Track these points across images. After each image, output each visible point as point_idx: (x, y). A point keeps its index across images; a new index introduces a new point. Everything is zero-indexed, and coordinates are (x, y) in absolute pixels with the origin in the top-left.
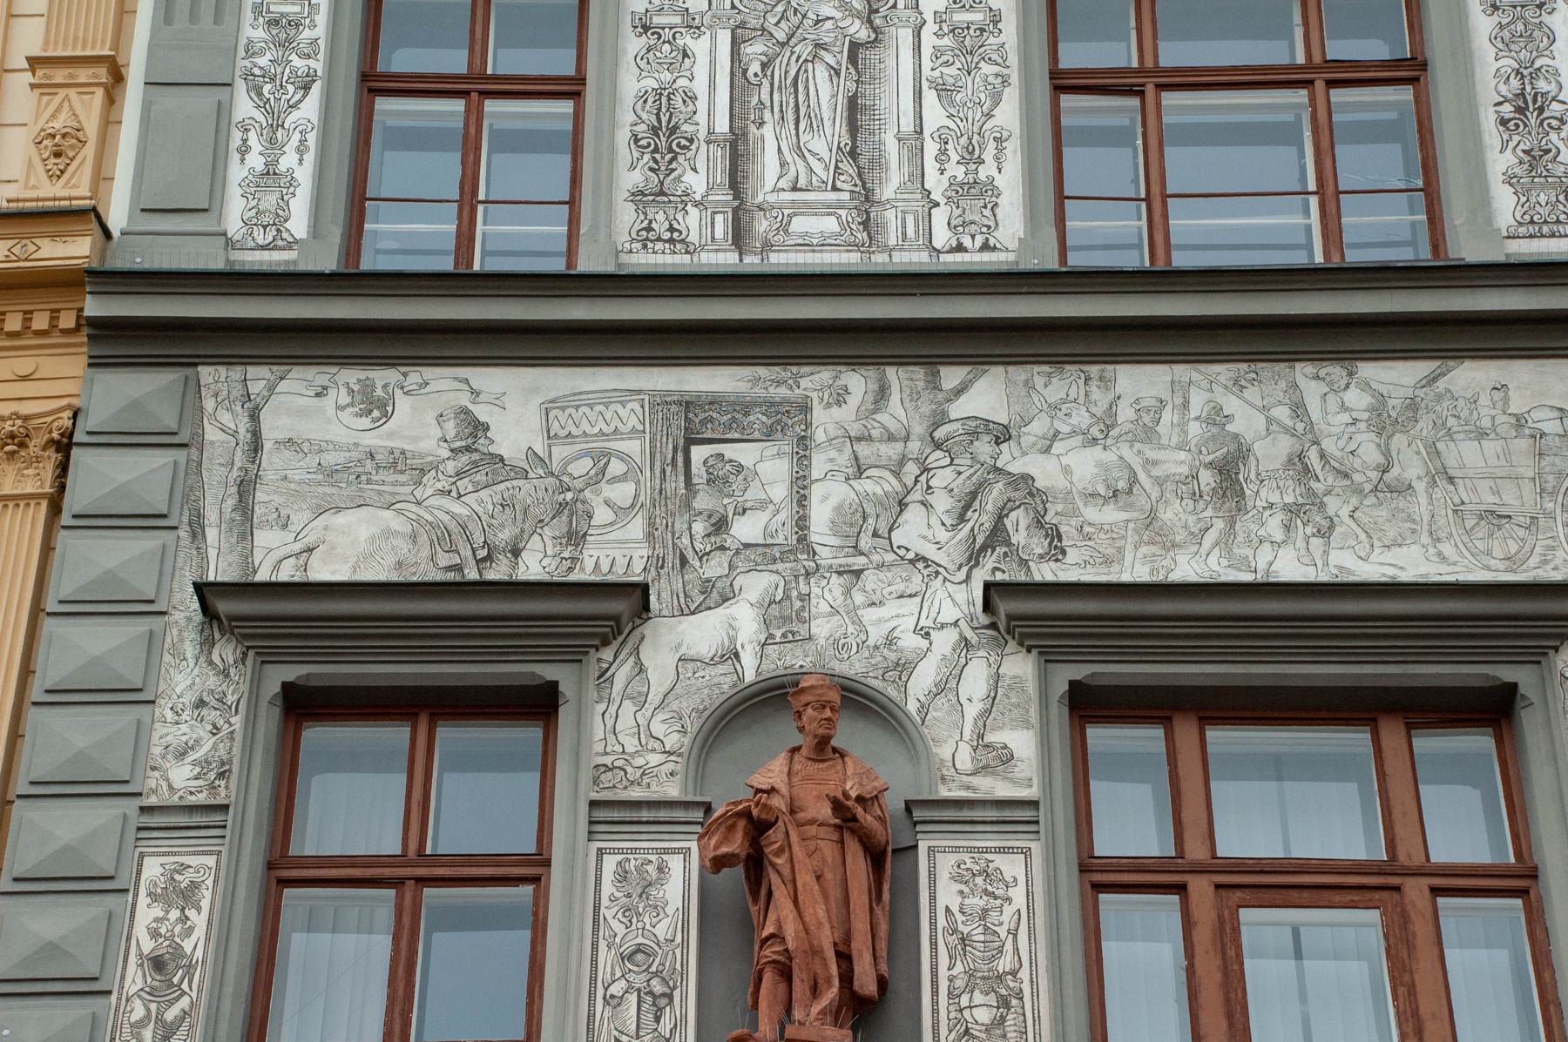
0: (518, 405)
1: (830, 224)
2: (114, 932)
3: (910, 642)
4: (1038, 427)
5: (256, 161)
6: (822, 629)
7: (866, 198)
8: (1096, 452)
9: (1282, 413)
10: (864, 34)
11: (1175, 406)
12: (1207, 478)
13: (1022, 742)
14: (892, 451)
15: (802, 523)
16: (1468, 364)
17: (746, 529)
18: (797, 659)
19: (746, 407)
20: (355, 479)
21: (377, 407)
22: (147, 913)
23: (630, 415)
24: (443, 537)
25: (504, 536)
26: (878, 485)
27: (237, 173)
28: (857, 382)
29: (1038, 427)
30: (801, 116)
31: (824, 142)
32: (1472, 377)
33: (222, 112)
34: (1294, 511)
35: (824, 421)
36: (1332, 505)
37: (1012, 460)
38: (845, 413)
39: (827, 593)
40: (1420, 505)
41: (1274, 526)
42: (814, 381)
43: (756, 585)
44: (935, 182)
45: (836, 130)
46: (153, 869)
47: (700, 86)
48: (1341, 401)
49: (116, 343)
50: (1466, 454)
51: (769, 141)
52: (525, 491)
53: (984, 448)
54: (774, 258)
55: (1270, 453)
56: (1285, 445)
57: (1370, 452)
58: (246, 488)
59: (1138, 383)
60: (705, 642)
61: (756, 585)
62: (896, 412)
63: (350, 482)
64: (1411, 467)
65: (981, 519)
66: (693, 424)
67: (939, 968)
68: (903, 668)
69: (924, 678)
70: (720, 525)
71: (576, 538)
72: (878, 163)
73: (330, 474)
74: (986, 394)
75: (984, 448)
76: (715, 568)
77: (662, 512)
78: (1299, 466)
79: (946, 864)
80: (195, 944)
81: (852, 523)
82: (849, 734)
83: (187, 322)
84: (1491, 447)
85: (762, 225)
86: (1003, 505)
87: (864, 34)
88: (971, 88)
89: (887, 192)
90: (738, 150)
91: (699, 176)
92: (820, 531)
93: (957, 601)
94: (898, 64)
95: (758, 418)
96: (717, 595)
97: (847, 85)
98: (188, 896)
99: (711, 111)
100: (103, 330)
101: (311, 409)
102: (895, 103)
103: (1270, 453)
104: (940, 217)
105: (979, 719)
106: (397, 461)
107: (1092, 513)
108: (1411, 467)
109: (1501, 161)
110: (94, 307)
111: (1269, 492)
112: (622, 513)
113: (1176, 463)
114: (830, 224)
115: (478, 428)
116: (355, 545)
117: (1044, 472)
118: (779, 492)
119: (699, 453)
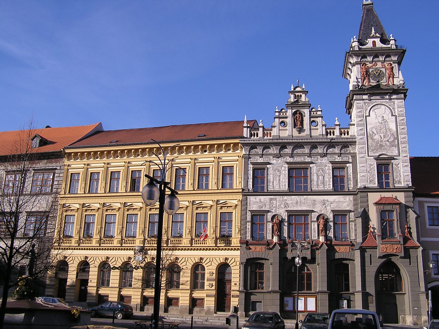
17: (274, 206)
18: (276, 213)
21: (256, 199)
23: (268, 199)
24: (259, 206)
26: (280, 203)
28: (279, 197)
30: (276, 180)
32: (309, 197)
35: (277, 199)
42: (277, 197)
43: (274, 209)
50: (308, 201)
55: (299, 201)
59: (293, 197)
61: (274, 209)
62: (281, 199)
64: (305, 202)
66: (271, 199)
74: (285, 197)
80: (250, 228)
81: (279, 205)
86: (286, 205)
88: (285, 178)
90: (273, 182)
91: (271, 184)
93: (284, 210)
99: (272, 180)
101: (252, 199)
102: (281, 179)
103: (299, 201)
108: (305, 202)
113: (294, 202)
116: (255, 208)
117: (288, 202)
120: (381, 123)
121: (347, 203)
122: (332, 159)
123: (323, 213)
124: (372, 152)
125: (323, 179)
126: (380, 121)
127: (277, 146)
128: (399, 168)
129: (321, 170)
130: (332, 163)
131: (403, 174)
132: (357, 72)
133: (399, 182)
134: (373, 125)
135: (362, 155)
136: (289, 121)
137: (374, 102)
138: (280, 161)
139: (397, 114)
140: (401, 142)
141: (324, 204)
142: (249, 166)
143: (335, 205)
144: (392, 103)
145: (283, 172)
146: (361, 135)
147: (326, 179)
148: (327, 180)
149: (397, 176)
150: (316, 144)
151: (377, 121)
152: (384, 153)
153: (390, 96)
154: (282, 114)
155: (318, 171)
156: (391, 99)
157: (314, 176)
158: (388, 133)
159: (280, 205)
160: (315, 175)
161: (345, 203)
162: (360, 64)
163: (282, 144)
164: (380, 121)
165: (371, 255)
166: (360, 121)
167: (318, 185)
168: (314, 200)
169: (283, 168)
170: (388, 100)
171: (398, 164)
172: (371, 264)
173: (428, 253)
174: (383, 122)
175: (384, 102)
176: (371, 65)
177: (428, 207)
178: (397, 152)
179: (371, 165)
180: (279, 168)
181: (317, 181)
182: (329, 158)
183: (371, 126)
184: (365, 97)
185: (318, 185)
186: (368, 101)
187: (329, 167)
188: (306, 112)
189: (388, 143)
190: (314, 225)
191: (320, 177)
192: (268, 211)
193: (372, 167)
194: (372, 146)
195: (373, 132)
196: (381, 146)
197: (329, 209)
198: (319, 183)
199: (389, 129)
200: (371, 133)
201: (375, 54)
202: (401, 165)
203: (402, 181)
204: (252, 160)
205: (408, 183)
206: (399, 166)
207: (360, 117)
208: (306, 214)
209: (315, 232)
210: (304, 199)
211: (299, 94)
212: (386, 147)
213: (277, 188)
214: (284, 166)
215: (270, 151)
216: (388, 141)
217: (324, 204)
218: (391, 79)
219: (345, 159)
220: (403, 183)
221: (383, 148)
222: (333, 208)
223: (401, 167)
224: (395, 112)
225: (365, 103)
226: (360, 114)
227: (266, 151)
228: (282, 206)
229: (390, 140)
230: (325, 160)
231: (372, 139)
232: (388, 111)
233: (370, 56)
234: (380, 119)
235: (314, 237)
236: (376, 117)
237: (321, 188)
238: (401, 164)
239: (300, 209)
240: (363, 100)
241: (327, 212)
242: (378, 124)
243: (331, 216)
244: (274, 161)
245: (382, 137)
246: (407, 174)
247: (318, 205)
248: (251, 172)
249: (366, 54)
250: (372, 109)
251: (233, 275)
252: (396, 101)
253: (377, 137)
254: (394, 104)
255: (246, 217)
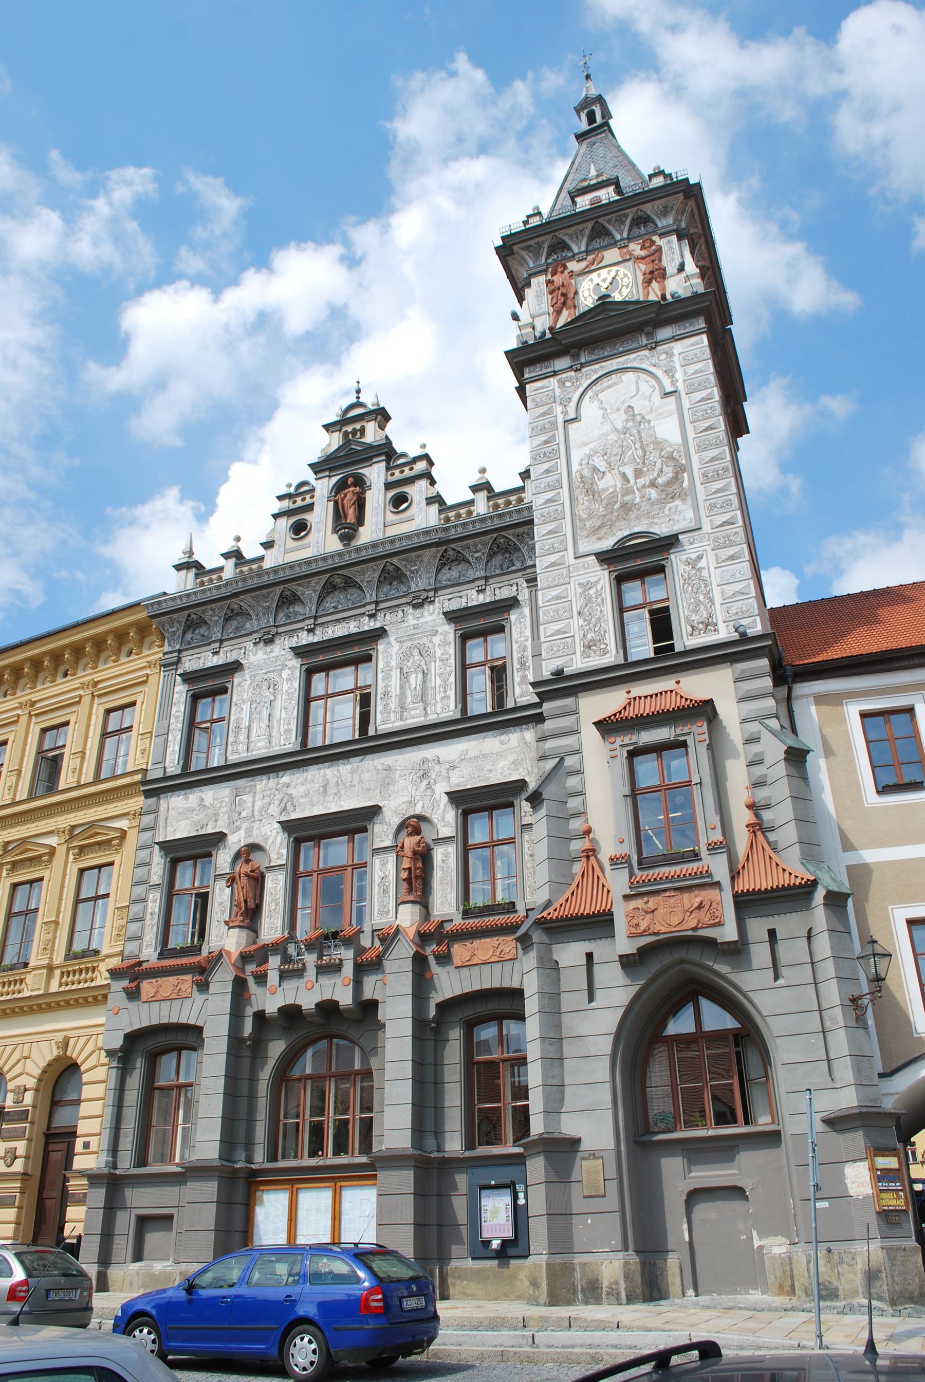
0: (209, 794)
1: (263, 743)
2: (145, 908)
3: (269, 833)
4: (294, 783)
5: (171, 749)
6: (254, 833)
7: (270, 736)
8: (304, 787)
9: (336, 772)
10: (272, 698)
11: (318, 775)
12: (322, 789)
13: (284, 851)
14: (269, 792)
15: (253, 811)
16: (369, 757)
17: (244, 814)
19: (246, 787)
20: (184, 814)
22: (150, 904)
24: (196, 824)
25: (205, 822)
27: (168, 752)
29: (294, 783)
30: (260, 720)
31: (264, 725)
33: (167, 741)
34: (335, 794)
36: (342, 792)
37: (290, 791)
38: (262, 786)
39: (256, 825)
40: (356, 789)
41: (331, 799)
43: (245, 825)
44: (282, 730)
45: (266, 721)
46: (151, 897)
47: (244, 716)
48: (345, 769)
49: (148, 794)
50: (366, 776)
51: (255, 726)
52: (210, 812)
53: (285, 788)
54: (254, 753)
55: (333, 781)
56: (336, 779)
57: (350, 779)
58: (166, 819)
60: (236, 840)
61: (245, 825)
63: (182, 815)
64: (356, 782)
65: (283, 805)
67: (267, 898)
68: (267, 839)
69: (270, 841)
70: (240, 814)
71: (216, 820)
72: (273, 728)
73: (179, 813)
74: (286, 778)
75: (285, 788)
76: (238, 823)
77: (231, 811)
78: (337, 784)
79: (270, 878)
80: (157, 910)
82: (256, 857)
83: (157, 788)
84: (370, 774)
85: (252, 746)
86: (288, 801)
87: (272, 698)
89: (273, 734)
90: (249, 729)
91: (242, 737)
92: (256, 813)
94: (278, 704)
95: (248, 789)
96: (238, 828)
97: (269, 711)
98: (155, 901)
99: (245, 723)
100: (144, 791)
101: (176, 802)
102: (277, 714)
103: (333, 781)
104: (282, 738)
105: (277, 848)
106: (190, 810)
107: (302, 800)
108: (356, 782)
109: (379, 708)
110: (142, 788)
111: (331, 791)
112: (224, 814)
113: (316, 787)
114: (263, 743)
115: (203, 799)
116: (180, 830)
118: (250, 805)
119: (238, 798)
120: (625, 431)
121: (511, 758)
122: (455, 605)
123: (418, 810)
124: (593, 539)
125: (424, 682)
126: (619, 426)
127: (266, 597)
128: (705, 573)
129: (416, 652)
130: (452, 617)
131: (722, 592)
132: (537, 296)
133: (709, 624)
134: (592, 446)
135: (553, 558)
136: (321, 517)
137: (595, 372)
138: (275, 653)
139: (680, 386)
140: (705, 475)
141: (424, 775)
142: (177, 689)
143: (466, 773)
144: (663, 356)
145: (286, 686)
146: (549, 488)
147: (435, 681)
148: (439, 682)
149: (698, 603)
150: (395, 560)
151: (608, 427)
152: (637, 530)
153: (650, 335)
154: (299, 499)
155: (407, 655)
156: (657, 344)
157: (387, 677)
158: (654, 456)
159: (264, 809)
160: (395, 674)
161: (501, 757)
162: (545, 271)
163: (278, 590)
164: (619, 426)
165: (589, 956)
166: (546, 442)
167: (403, 708)
168: (388, 769)
169: (285, 674)
170: (646, 352)
171: (700, 558)
172: (591, 998)
173: (886, 920)
174: (630, 424)
175: (634, 360)
176: (583, 264)
177: (864, 715)
178: (690, 514)
179: (587, 586)
180: (271, 675)
181: (402, 695)
182: (446, 603)
183: (586, 450)
184: (563, 363)
185: (403, 708)
186: (572, 373)
187: (445, 634)
188: (375, 474)
189: (653, 493)
190: (384, 864)
191: (412, 678)
192: (220, 838)
193: (592, 591)
194: (590, 517)
195: (595, 470)
196: (627, 508)
197: (441, 788)
198: (409, 699)
199: (658, 444)
200: (586, 472)
201: (590, 225)
202: (709, 562)
203: (719, 617)
204: (190, 663)
205: (744, 622)
206: (702, 563)
207: (544, 430)
208: (356, 822)
209: (385, 891)
210: (353, 772)
211: (358, 426)
212: (645, 506)
213: (260, 749)
214: (290, 664)
215: (248, 625)
216: (653, 484)
217: (424, 775)
218: (654, 284)
219: (505, 593)
220: (722, 627)
221: (633, 515)
222: (458, 785)
223: (713, 564)
224: (674, 383)
225: (562, 383)
226: (545, 421)
227: (237, 628)
228: (274, 810)
229: (660, 481)
230: (432, 615)
231: (592, 492)
232: (647, 386)
233: (577, 237)
234: (619, 420)
235: (381, 914)
236: (605, 416)
237: (415, 718)
238: (711, 555)
239: (334, 808)
240: (555, 373)
241: (434, 804)
242: (613, 436)
243: (445, 821)
244: (255, 657)
245: (630, 475)
246: (738, 587)
247: (401, 783)
248: (179, 709)
249: (561, 235)
250: (590, 393)
251: (85, 1109)
252: (677, 347)
253: (609, 482)
254: (670, 354)
255: (149, 871)
